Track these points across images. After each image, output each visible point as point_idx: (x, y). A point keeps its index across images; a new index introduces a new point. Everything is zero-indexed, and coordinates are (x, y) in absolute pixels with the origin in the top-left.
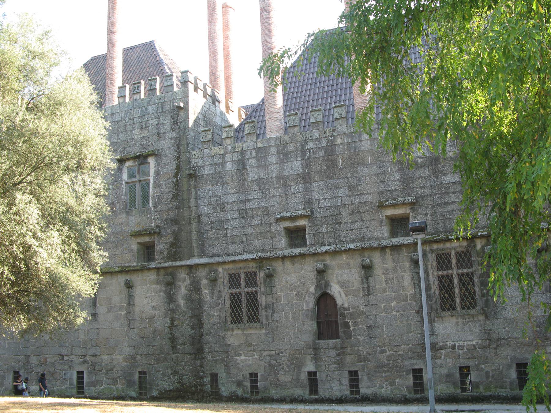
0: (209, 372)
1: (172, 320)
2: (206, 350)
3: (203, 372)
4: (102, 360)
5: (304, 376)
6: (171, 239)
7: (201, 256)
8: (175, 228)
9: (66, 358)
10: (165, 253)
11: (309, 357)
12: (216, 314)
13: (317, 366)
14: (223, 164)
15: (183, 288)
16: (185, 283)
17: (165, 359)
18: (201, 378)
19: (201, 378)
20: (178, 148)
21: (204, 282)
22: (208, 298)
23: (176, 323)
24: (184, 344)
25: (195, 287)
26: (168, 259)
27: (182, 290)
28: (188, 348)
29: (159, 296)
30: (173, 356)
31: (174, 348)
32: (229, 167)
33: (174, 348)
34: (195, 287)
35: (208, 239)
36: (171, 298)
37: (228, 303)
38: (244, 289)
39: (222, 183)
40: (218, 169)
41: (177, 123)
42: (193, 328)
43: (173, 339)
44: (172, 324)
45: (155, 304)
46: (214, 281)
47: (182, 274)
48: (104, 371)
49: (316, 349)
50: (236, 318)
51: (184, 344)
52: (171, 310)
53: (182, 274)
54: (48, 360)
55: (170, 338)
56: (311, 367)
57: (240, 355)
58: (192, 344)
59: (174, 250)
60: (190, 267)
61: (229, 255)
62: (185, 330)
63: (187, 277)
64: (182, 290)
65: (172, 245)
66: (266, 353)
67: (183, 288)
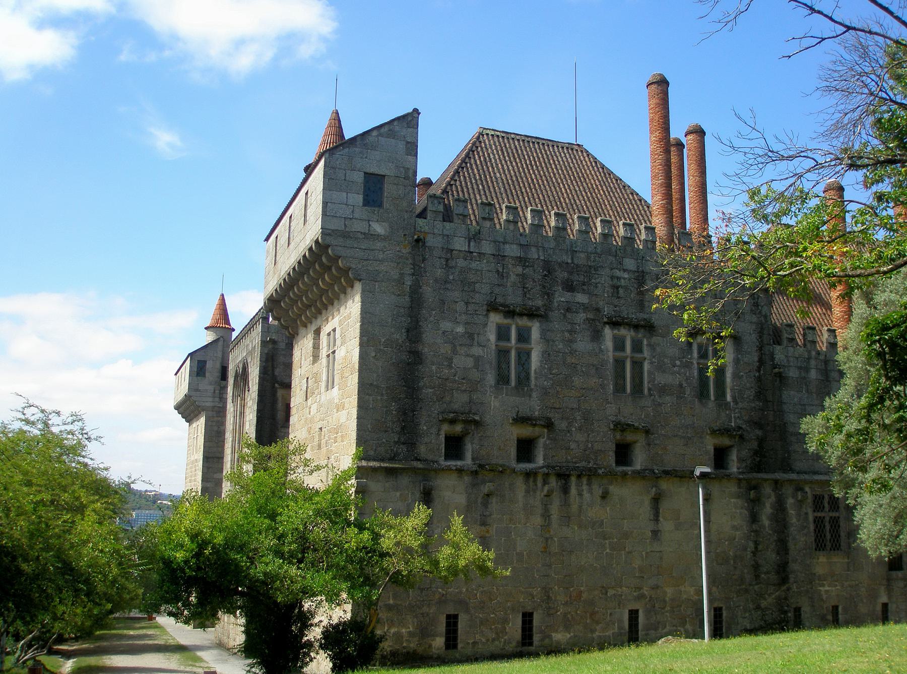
0: (794, 606)
1: (756, 543)
2: (792, 580)
3: (788, 606)
4: (666, 592)
5: (879, 608)
6: (755, 445)
7: (785, 471)
8: (759, 433)
9: (611, 592)
10: (749, 462)
11: (883, 588)
12: (802, 539)
13: (890, 597)
14: (807, 370)
15: (768, 505)
16: (770, 500)
17: (746, 591)
18: (786, 612)
19: (786, 612)
20: (761, 337)
21: (790, 501)
22: (794, 520)
23: (760, 547)
24: (767, 573)
25: (780, 506)
26: (751, 468)
27: (768, 509)
28: (773, 577)
29: (741, 513)
30: (756, 587)
31: (757, 577)
32: (813, 374)
33: (757, 577)
34: (780, 506)
35: (795, 452)
36: (754, 518)
37: (812, 527)
38: (827, 515)
39: (807, 391)
40: (803, 374)
41: (758, 306)
42: (778, 554)
43: (756, 567)
44: (756, 548)
45: (736, 523)
46: (801, 502)
47: (767, 490)
48: (668, 608)
49: (889, 580)
50: (819, 545)
51: (767, 573)
52: (756, 531)
53: (767, 490)
54: (585, 596)
55: (753, 566)
56: (884, 599)
57: (823, 585)
58: (778, 573)
59: (758, 459)
60: (776, 482)
61: (815, 473)
62: (770, 556)
63: (773, 494)
64: (768, 509)
65: (756, 453)
66: (846, 584)
67: (768, 505)
